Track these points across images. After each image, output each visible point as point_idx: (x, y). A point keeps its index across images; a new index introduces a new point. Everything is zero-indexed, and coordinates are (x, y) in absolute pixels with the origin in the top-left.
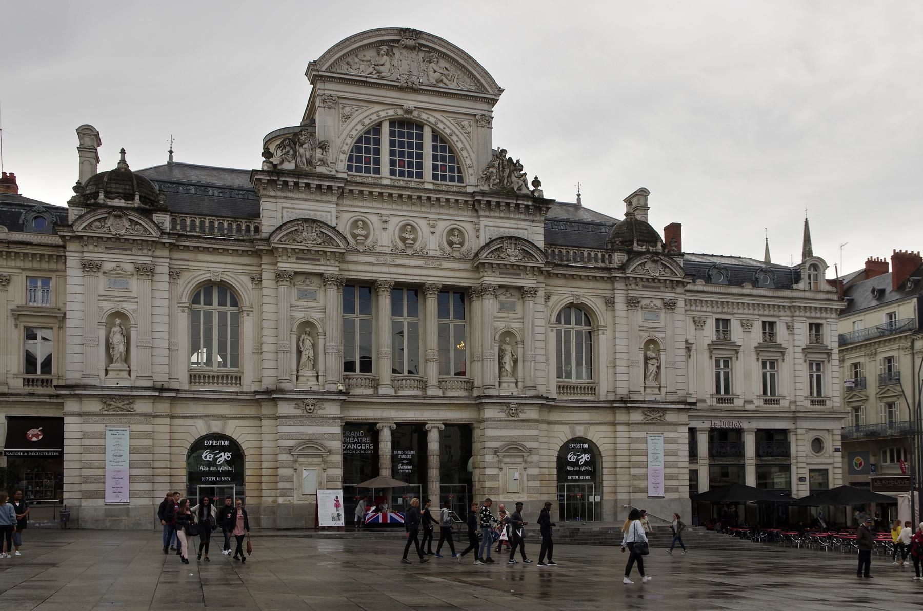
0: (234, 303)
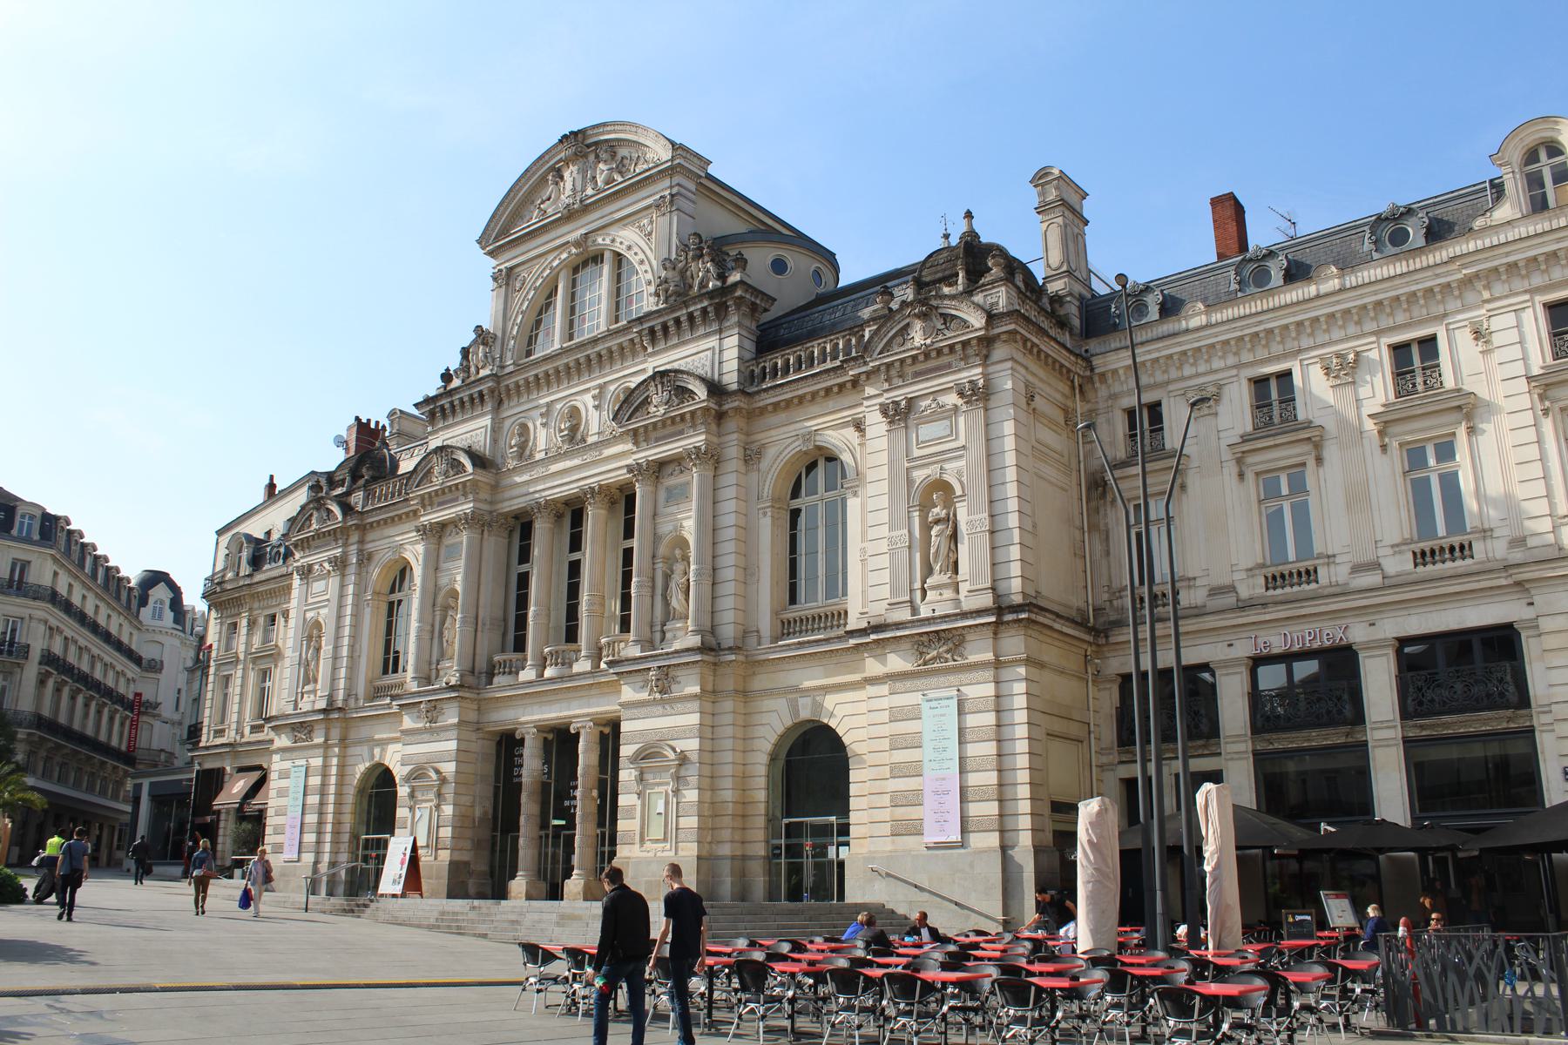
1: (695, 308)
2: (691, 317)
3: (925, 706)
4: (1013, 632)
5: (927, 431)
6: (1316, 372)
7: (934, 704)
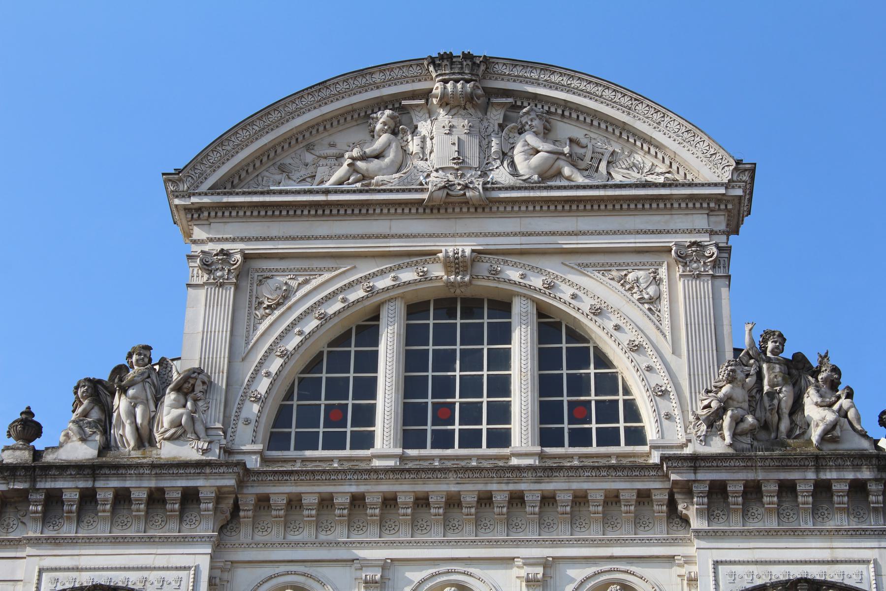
1: (839, 477)
2: (822, 489)
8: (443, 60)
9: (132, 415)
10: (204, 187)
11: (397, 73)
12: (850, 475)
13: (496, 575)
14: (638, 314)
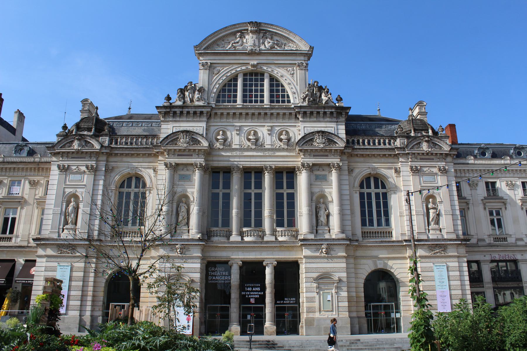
0: (144, 185)
1: (328, 111)
2: (325, 113)
3: (435, 268)
4: (461, 247)
5: (425, 178)
6: (504, 184)
7: (438, 267)
8: (251, 23)
9: (189, 96)
10: (202, 49)
11: (241, 25)
12: (330, 111)
13: (262, 129)
14: (290, 77)
